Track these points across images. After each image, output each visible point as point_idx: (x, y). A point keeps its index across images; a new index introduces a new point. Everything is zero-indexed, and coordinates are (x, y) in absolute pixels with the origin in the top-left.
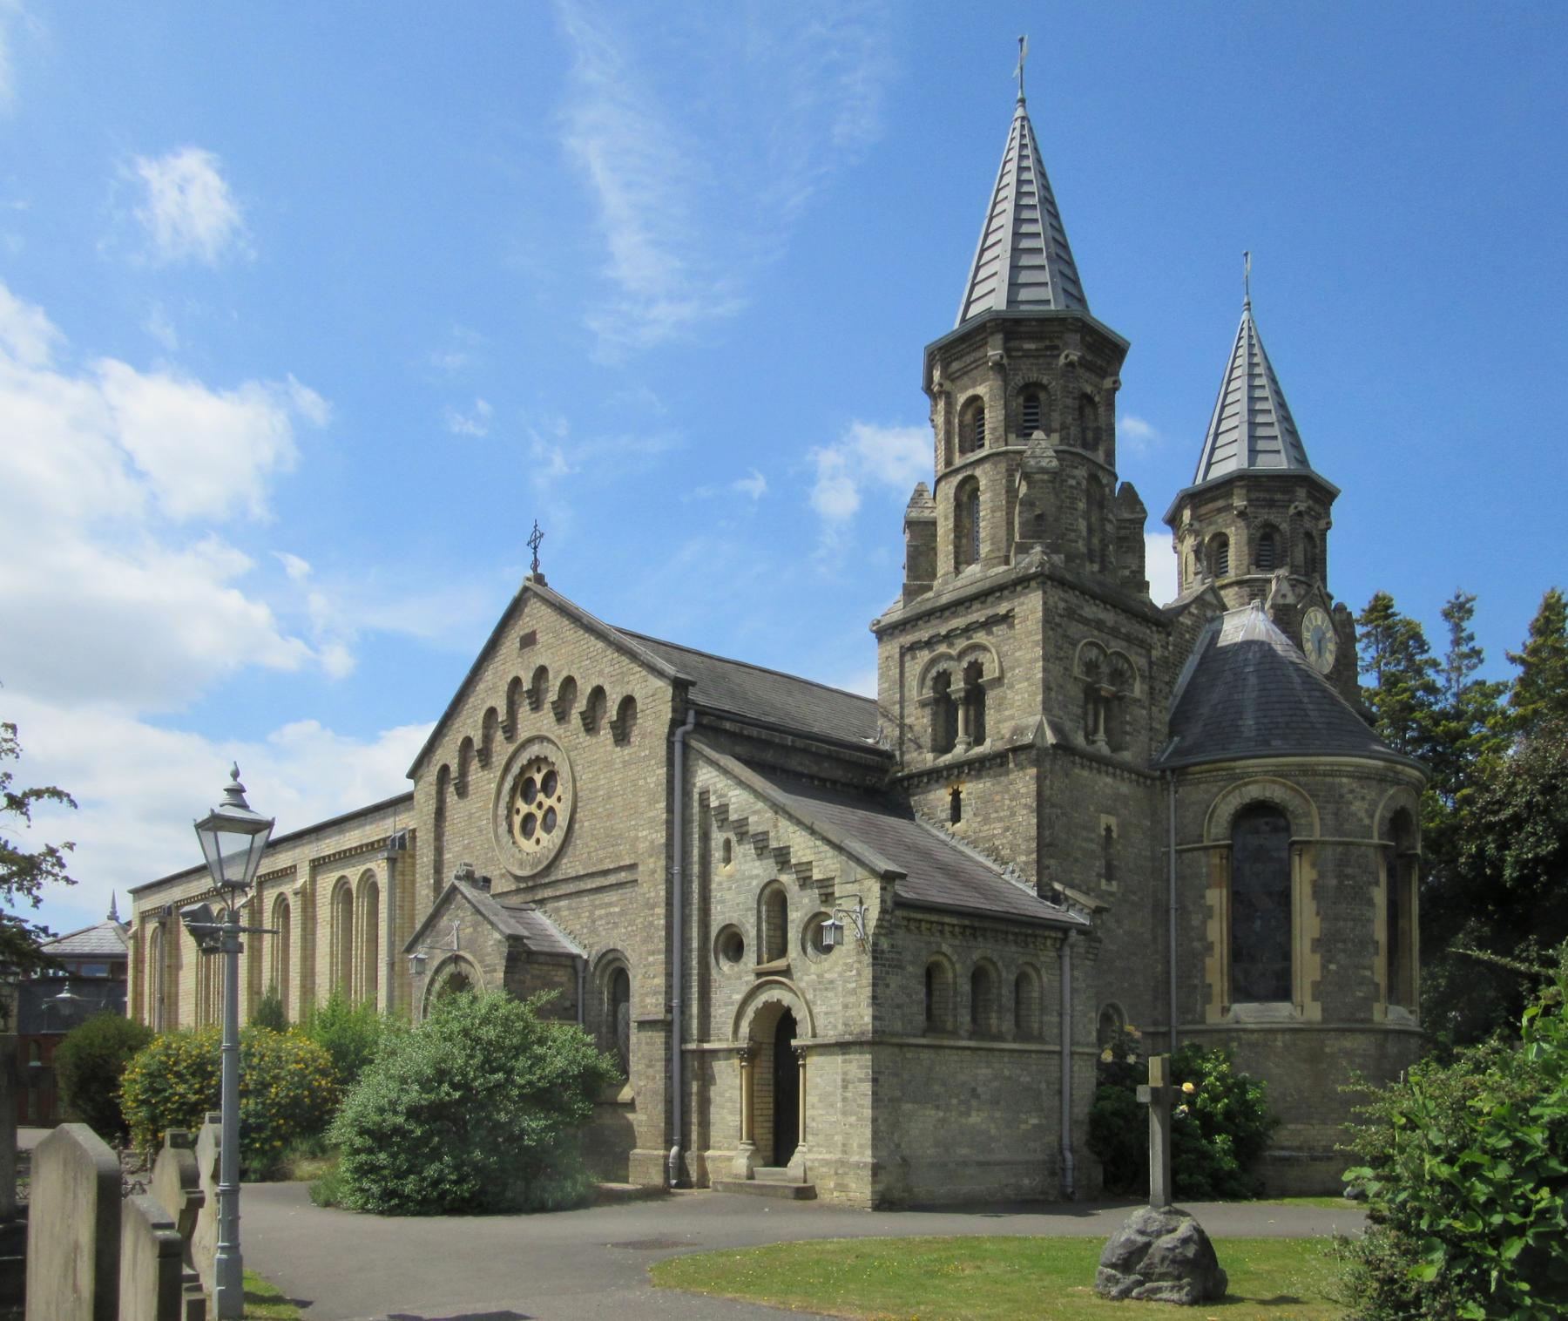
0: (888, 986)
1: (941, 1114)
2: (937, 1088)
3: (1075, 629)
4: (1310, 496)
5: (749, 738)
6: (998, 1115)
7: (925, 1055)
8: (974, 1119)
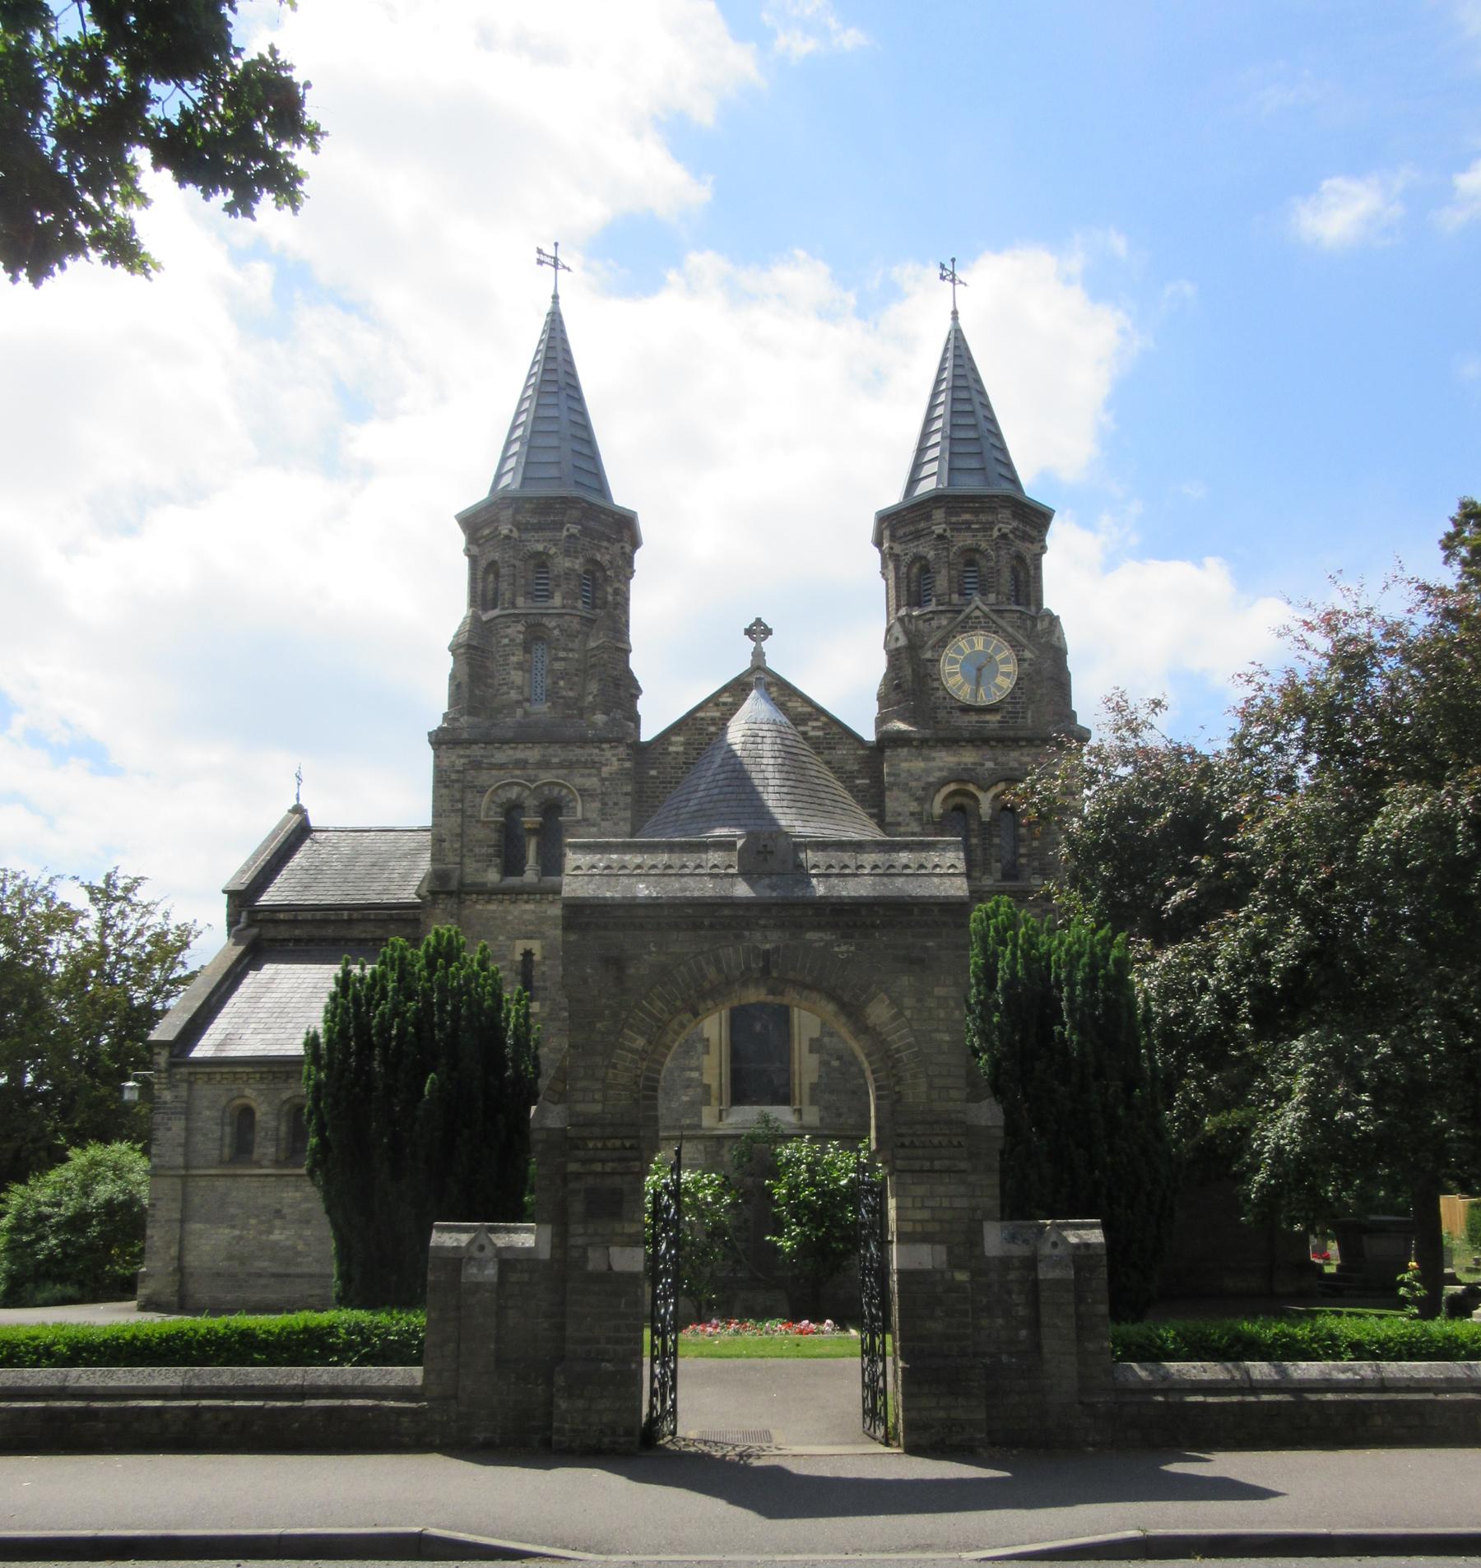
0: (169, 1129)
1: (237, 1232)
2: (232, 1210)
3: (484, 777)
4: (1015, 516)
5: (306, 922)
6: (307, 1232)
7: (221, 1184)
8: (276, 1236)
